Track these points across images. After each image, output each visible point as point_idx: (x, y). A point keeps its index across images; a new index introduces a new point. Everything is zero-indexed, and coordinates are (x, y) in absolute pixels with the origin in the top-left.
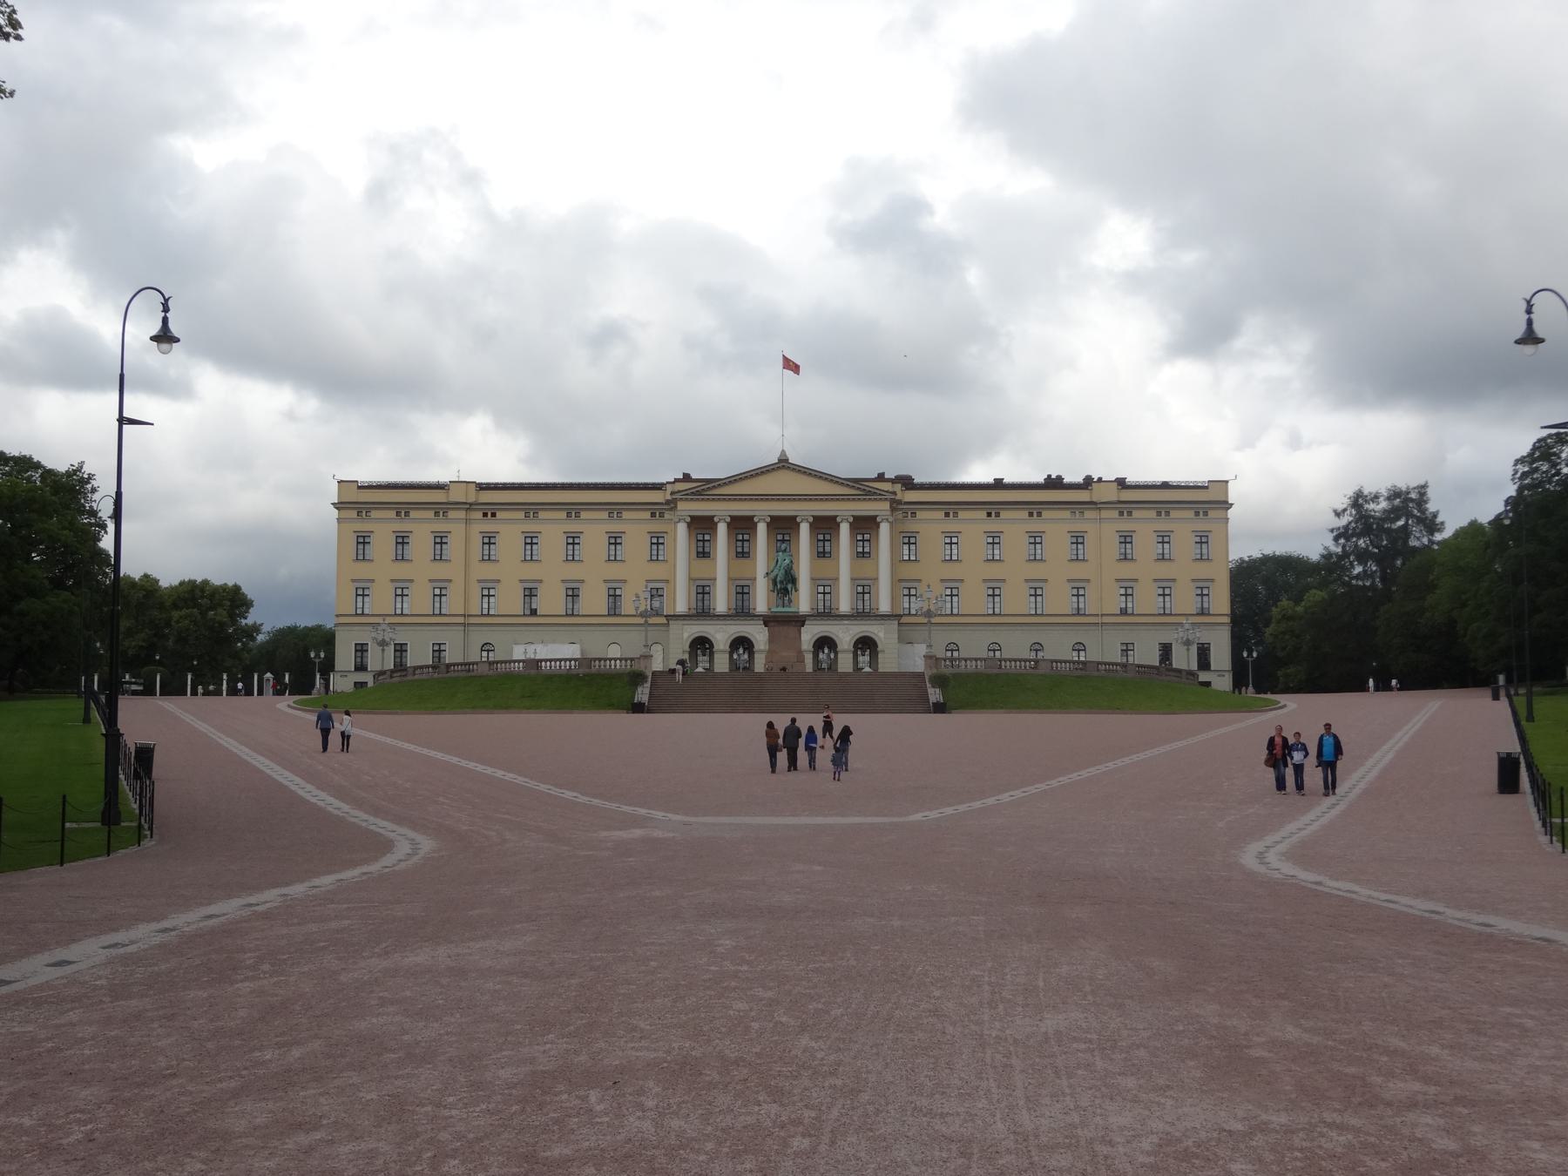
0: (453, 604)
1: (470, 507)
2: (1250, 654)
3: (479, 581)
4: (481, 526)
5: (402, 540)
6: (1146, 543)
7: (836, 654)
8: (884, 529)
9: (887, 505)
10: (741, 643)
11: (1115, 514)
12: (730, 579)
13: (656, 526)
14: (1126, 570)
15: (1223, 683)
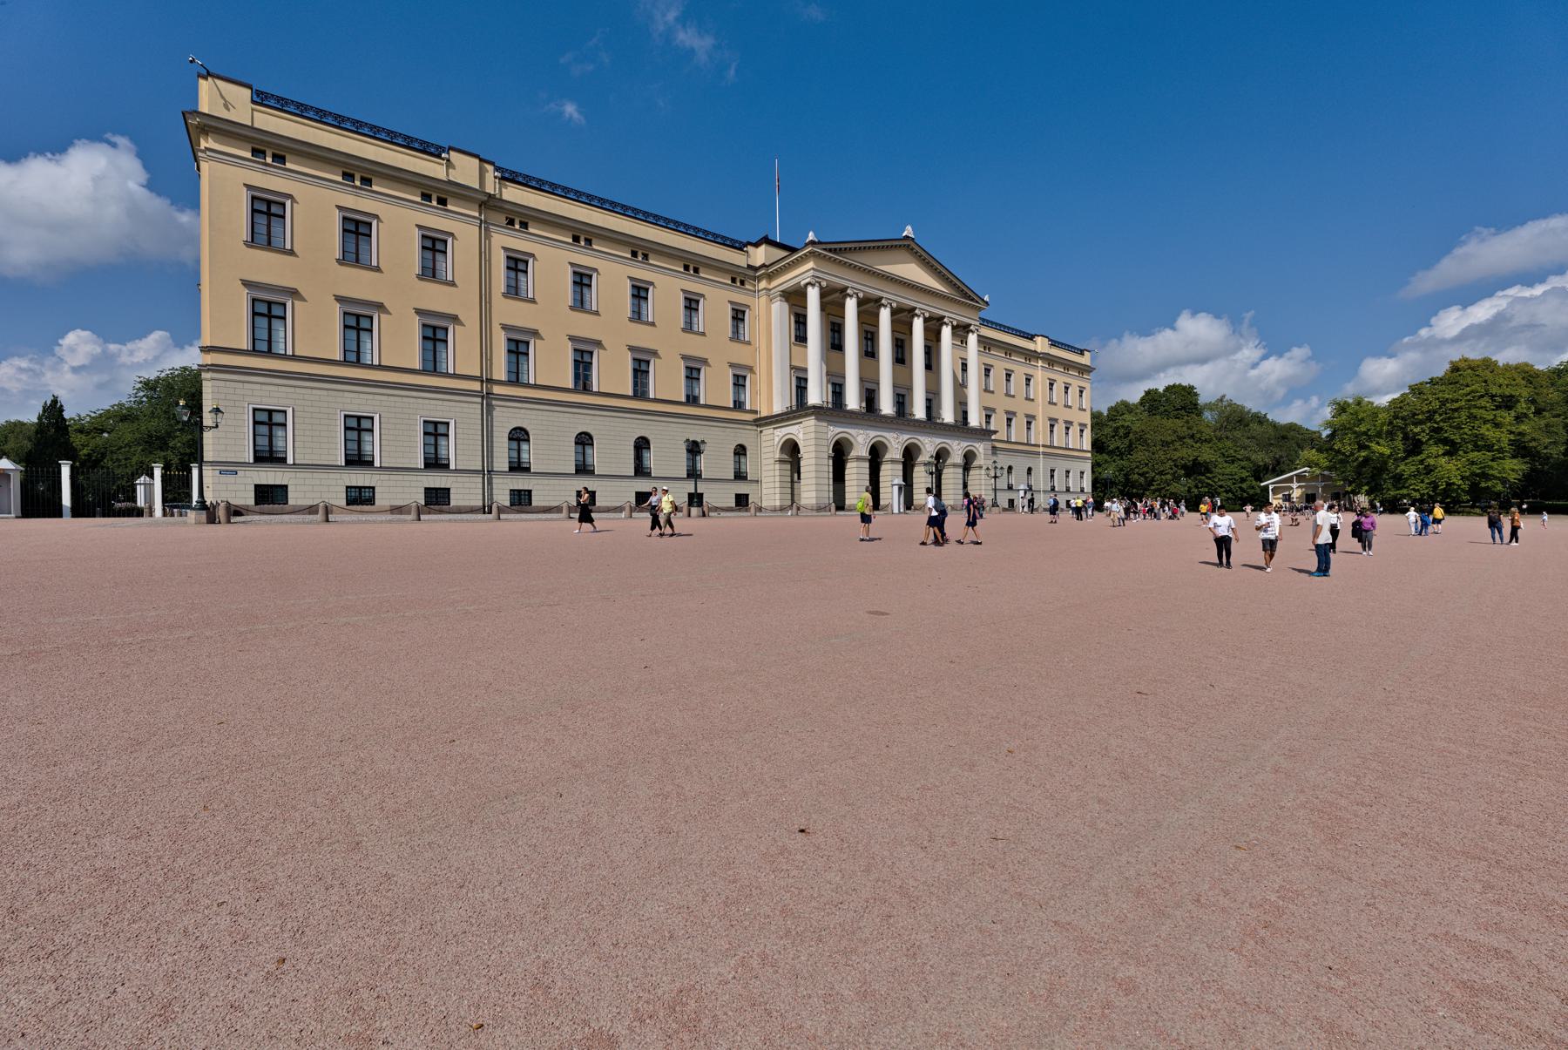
1: (489, 203)
3: (505, 327)
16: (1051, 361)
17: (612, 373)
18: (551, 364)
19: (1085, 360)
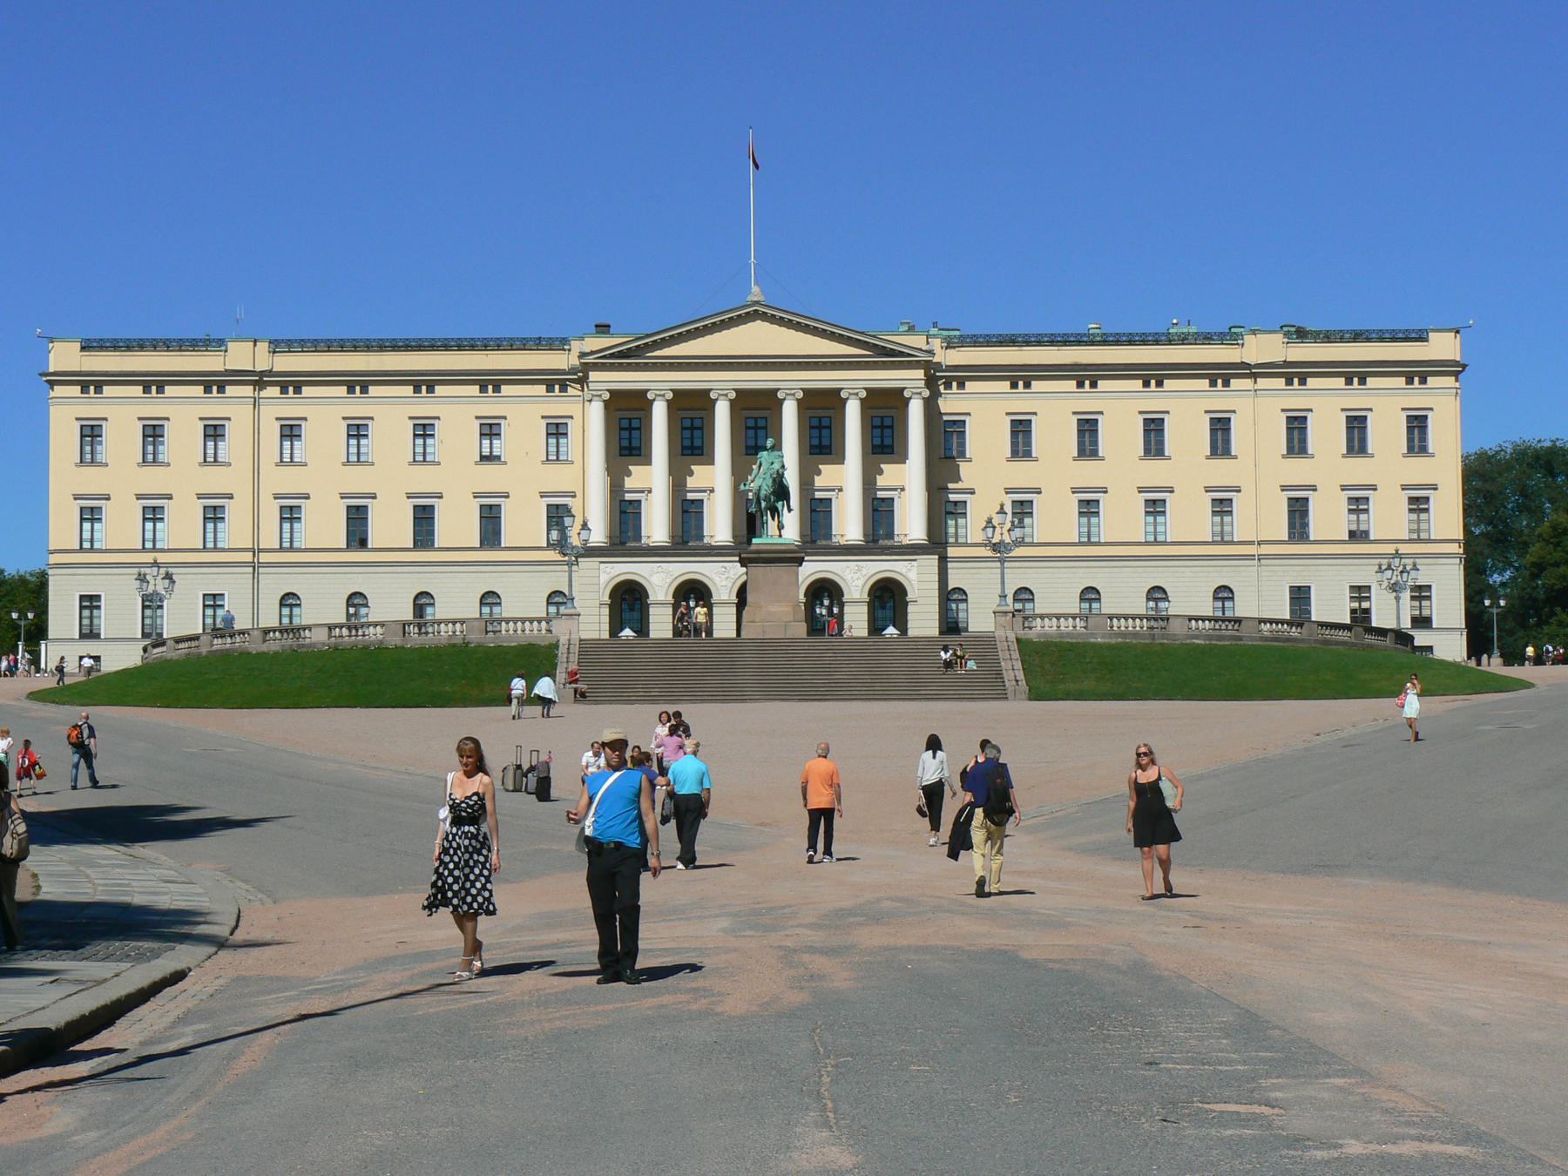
0: (235, 531)
1: (260, 380)
2: (1495, 604)
4: (277, 408)
5: (153, 433)
6: (1326, 432)
7: (842, 606)
9: (920, 374)
10: (693, 592)
13: (559, 406)
14: (1298, 471)
16: (1295, 374)
17: (391, 526)
18: (324, 525)
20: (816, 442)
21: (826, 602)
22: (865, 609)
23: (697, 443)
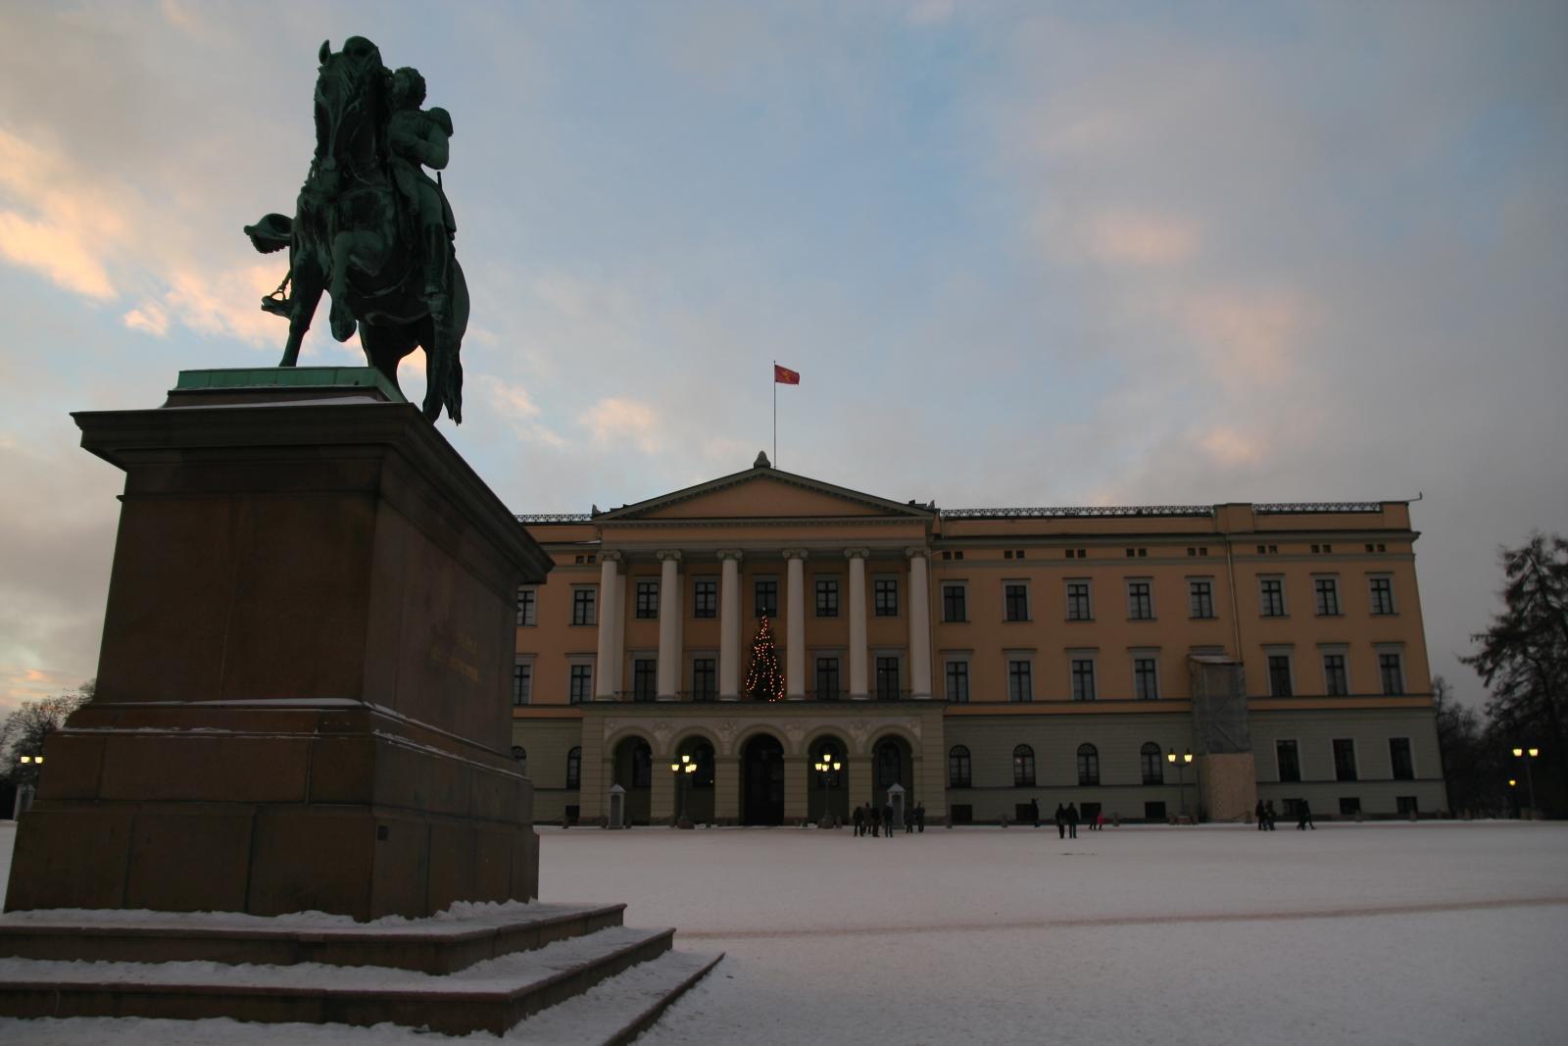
6: (1300, 593)
8: (918, 566)
9: (919, 532)
11: (1253, 550)
12: (684, 650)
13: (582, 576)
15: (1433, 795)
19: (1391, 521)
20: (822, 605)
21: (827, 758)
22: (869, 765)
23: (711, 606)
